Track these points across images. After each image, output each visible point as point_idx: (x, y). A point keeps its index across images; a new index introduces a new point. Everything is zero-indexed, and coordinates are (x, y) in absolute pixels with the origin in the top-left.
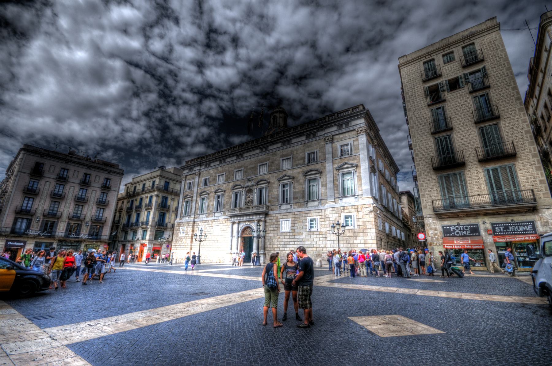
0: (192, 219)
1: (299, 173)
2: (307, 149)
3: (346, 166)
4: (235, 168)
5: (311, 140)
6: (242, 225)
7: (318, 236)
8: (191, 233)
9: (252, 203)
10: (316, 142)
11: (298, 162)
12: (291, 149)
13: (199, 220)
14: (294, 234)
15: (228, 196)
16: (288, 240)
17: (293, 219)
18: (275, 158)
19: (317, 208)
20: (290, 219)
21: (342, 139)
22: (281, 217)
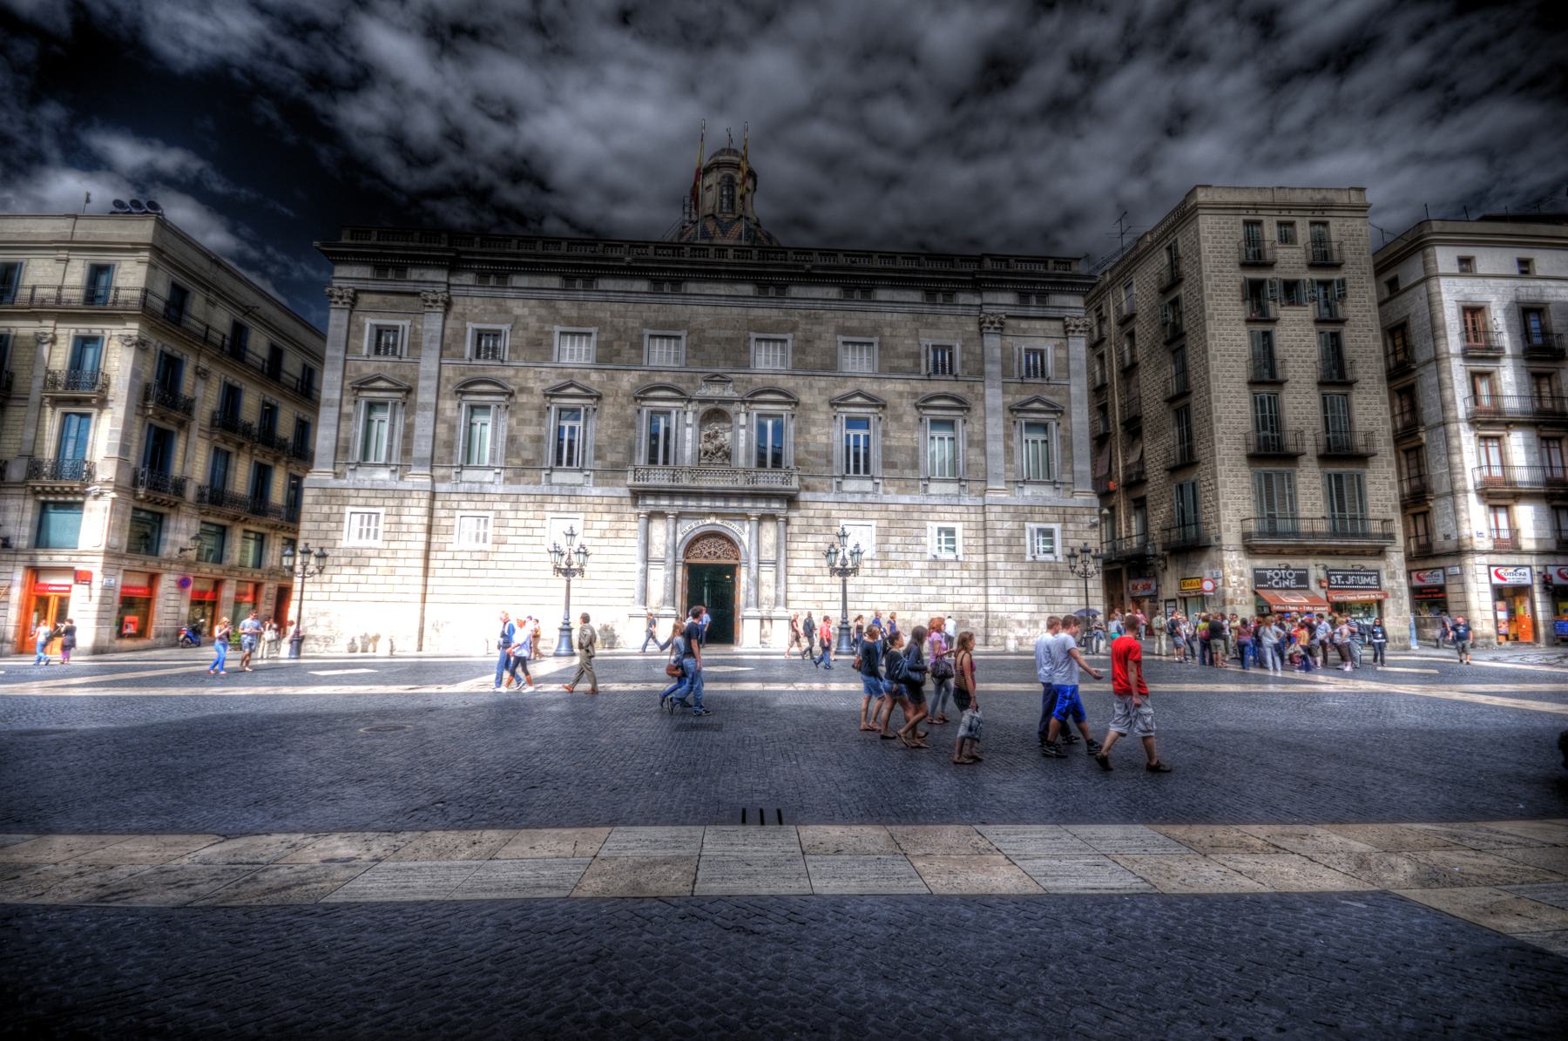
0: (418, 479)
1: (901, 395)
2: (928, 331)
3: (1036, 405)
4: (646, 324)
5: (938, 309)
6: (688, 527)
7: (956, 574)
8: (423, 537)
9: (728, 455)
10: (953, 319)
11: (896, 362)
12: (872, 316)
13: (461, 488)
14: (886, 564)
15: (615, 417)
16: (868, 581)
17: (884, 523)
18: (817, 329)
19: (955, 501)
20: (874, 523)
21: (1024, 334)
22: (845, 514)
